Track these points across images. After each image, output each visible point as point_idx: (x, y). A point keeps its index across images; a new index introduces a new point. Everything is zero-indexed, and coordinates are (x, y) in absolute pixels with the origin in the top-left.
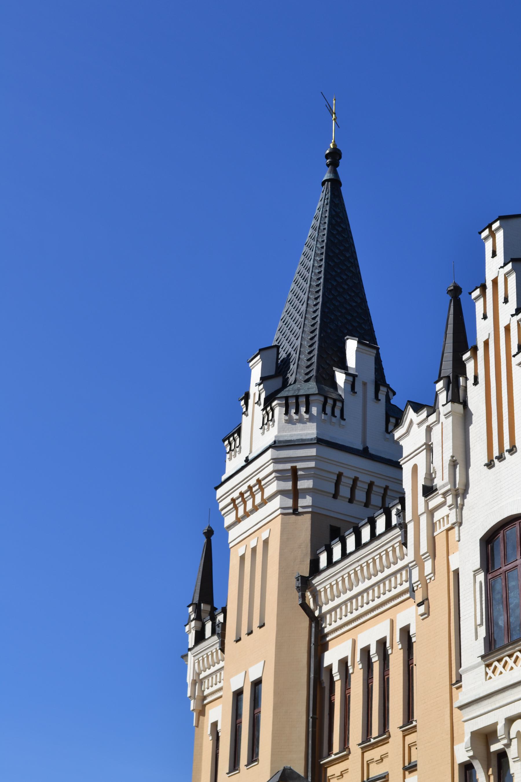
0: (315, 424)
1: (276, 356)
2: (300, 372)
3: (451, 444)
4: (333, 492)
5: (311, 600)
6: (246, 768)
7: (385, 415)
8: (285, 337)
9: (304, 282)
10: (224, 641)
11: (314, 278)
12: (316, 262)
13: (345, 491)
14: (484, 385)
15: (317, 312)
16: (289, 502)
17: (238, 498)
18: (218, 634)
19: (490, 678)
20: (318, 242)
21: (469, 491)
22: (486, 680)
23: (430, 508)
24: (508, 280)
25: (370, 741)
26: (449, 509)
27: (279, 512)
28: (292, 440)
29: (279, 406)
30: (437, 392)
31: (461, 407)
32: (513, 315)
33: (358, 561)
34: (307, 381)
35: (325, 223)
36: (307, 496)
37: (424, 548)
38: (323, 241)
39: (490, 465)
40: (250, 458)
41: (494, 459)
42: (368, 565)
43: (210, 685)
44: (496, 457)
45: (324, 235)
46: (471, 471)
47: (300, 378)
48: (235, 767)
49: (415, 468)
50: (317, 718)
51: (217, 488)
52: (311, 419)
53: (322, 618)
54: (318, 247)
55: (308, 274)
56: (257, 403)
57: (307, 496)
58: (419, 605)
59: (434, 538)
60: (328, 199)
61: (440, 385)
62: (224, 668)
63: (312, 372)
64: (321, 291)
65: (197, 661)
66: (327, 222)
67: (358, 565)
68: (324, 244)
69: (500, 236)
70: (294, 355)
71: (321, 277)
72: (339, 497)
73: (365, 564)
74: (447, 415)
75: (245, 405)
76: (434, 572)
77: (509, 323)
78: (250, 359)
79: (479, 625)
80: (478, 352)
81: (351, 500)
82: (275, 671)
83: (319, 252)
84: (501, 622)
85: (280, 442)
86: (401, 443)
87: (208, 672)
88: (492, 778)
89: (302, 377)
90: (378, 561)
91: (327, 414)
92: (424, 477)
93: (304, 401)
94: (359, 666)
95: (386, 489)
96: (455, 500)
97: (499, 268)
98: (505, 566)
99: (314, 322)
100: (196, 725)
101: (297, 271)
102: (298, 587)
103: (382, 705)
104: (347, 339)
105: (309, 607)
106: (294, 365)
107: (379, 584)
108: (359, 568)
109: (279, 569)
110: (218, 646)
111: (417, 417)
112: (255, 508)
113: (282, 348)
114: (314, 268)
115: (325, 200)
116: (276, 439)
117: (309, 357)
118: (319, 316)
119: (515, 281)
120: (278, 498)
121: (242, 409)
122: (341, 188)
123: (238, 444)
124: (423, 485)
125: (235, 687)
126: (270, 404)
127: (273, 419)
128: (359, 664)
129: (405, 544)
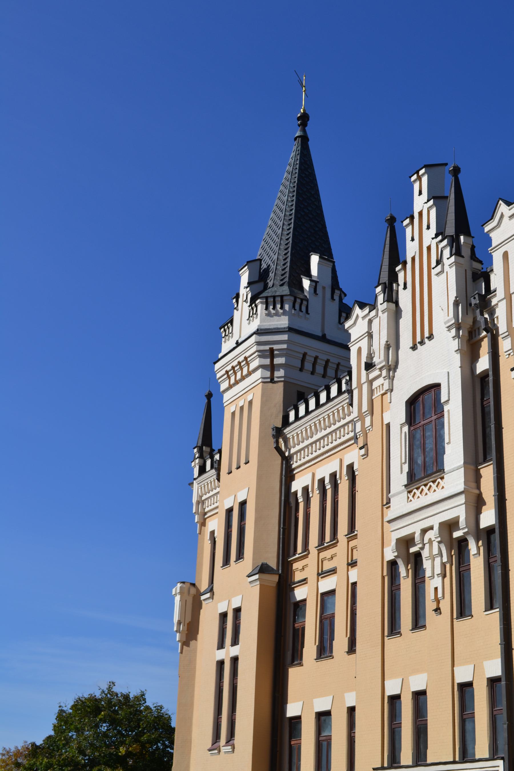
0: (287, 317)
1: (259, 266)
2: (276, 279)
3: (386, 333)
4: (300, 367)
5: (283, 445)
6: (234, 563)
7: (338, 311)
8: (266, 253)
9: (280, 213)
10: (220, 473)
11: (288, 209)
12: (289, 198)
13: (308, 366)
14: (411, 289)
15: (290, 235)
16: (268, 374)
17: (230, 371)
18: (215, 468)
19: (411, 501)
20: (291, 183)
21: (399, 367)
22: (408, 502)
23: (370, 379)
24: (430, 212)
25: (324, 545)
26: (384, 380)
27: (260, 381)
28: (270, 328)
29: (261, 304)
30: (376, 294)
31: (394, 305)
32: (433, 239)
33: (317, 417)
34: (282, 285)
35: (296, 168)
36: (281, 370)
37: (365, 408)
38: (295, 182)
39: (414, 348)
40: (240, 341)
41: (417, 344)
42: (324, 420)
43: (209, 504)
44: (419, 342)
45: (295, 177)
46: (400, 352)
47: (277, 283)
48: (227, 562)
49: (360, 350)
50: (286, 529)
51: (215, 363)
52: (284, 314)
53: (291, 457)
54: (291, 187)
55: (283, 207)
56: (245, 301)
57: (281, 370)
58: (361, 448)
59: (372, 400)
60: (298, 150)
61: (379, 289)
62: (220, 492)
63: (285, 279)
64: (293, 219)
65: (200, 487)
66: (298, 168)
67: (317, 420)
68: (296, 184)
69: (425, 180)
70: (273, 266)
71: (293, 209)
72: (304, 371)
73: (322, 419)
74: (383, 311)
75: (236, 303)
76: (372, 425)
77: (430, 244)
78: (240, 269)
79: (404, 463)
80: (407, 265)
81: (313, 373)
82: (256, 495)
83: (292, 190)
84: (420, 461)
85: (261, 330)
86: (350, 331)
87: (208, 495)
88: (410, 571)
89: (278, 283)
90: (331, 417)
91: (296, 310)
92: (366, 356)
93: (278, 300)
94: (317, 492)
95: (338, 365)
96: (388, 373)
97: (424, 204)
98: (423, 421)
99: (287, 242)
100: (199, 533)
101: (276, 204)
102: (273, 435)
103: (333, 519)
104: (312, 255)
105: (281, 450)
106: (272, 273)
107: (332, 433)
108: (318, 421)
109: (260, 422)
110: (215, 477)
111: (362, 312)
112: (243, 378)
113: (264, 261)
114: (288, 202)
115: (296, 151)
117: (283, 268)
118: (291, 237)
119: (435, 213)
120: (260, 370)
121: (234, 305)
122: (309, 143)
123: (230, 331)
124: (365, 362)
125: (227, 506)
126: (255, 302)
127: (256, 313)
128: (317, 490)
129: (351, 404)
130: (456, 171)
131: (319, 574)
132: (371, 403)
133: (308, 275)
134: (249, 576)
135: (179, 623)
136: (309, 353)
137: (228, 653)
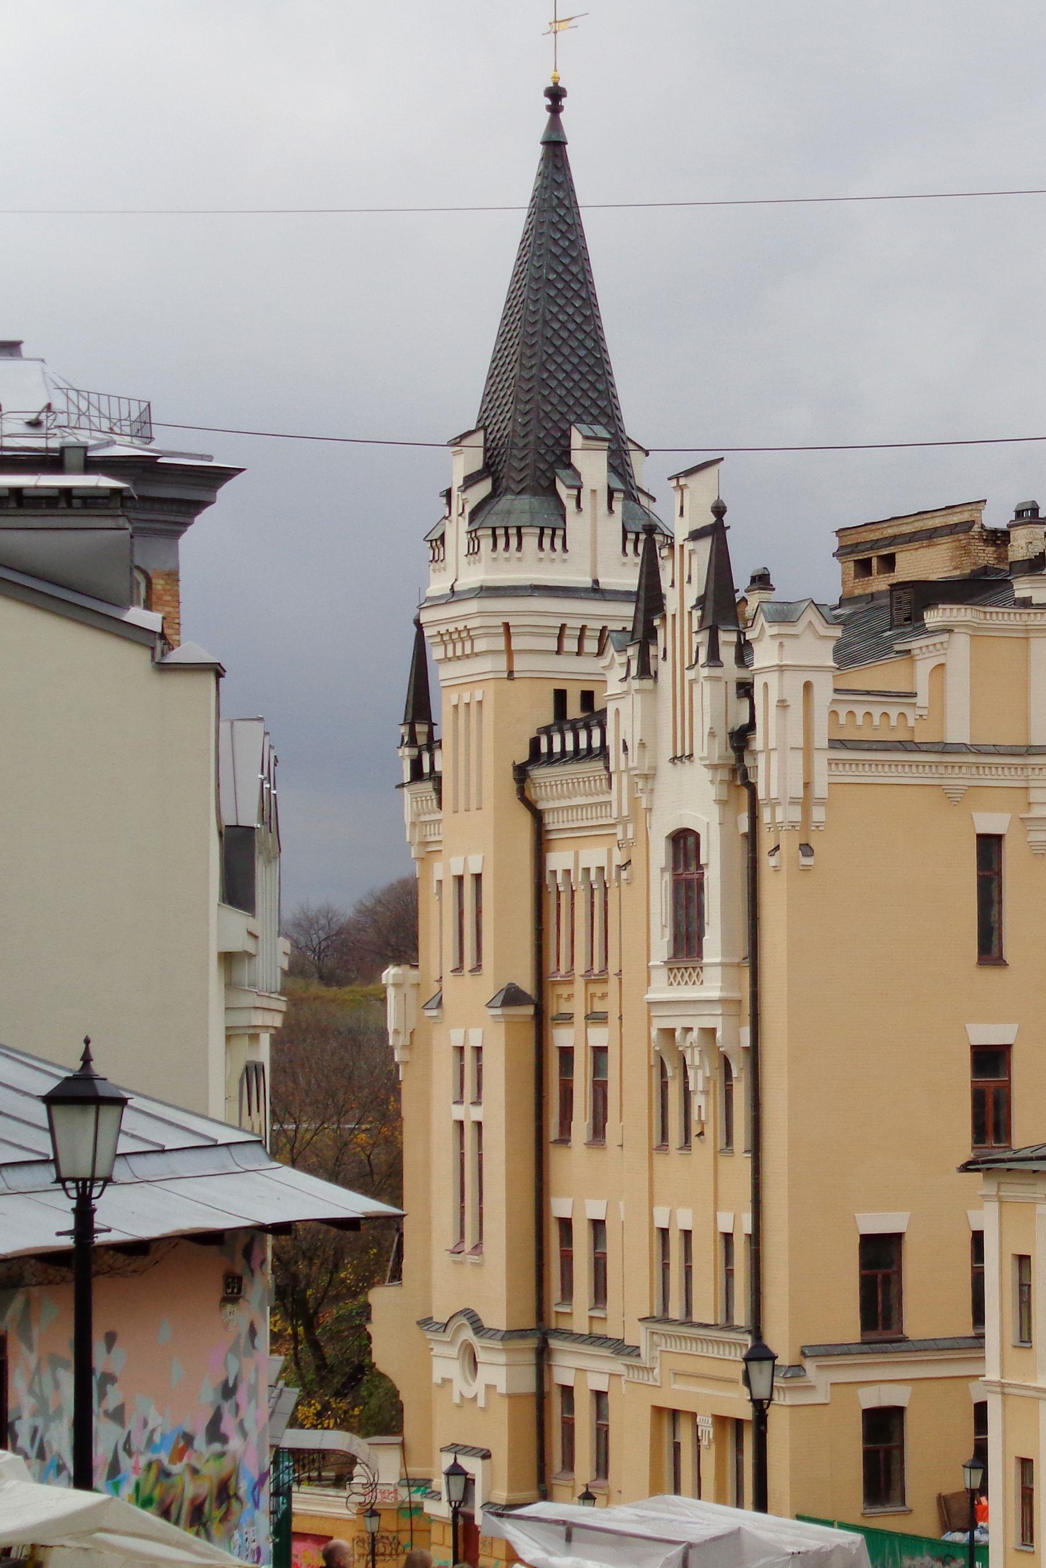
13: (570, 645)
16: (502, 663)
34: (519, 493)
37: (625, 813)
56: (460, 515)
81: (579, 653)
116: (485, 584)
130: (719, 510)
131: (587, 1017)
132: (634, 801)
133: (569, 466)
134: (489, 1005)
135: (396, 1032)
136: (570, 623)
137: (467, 1113)
